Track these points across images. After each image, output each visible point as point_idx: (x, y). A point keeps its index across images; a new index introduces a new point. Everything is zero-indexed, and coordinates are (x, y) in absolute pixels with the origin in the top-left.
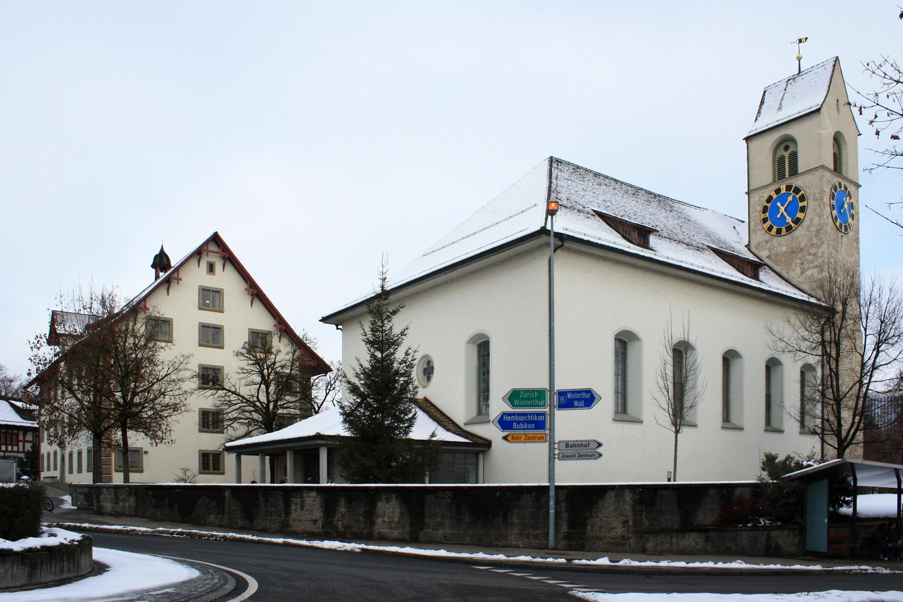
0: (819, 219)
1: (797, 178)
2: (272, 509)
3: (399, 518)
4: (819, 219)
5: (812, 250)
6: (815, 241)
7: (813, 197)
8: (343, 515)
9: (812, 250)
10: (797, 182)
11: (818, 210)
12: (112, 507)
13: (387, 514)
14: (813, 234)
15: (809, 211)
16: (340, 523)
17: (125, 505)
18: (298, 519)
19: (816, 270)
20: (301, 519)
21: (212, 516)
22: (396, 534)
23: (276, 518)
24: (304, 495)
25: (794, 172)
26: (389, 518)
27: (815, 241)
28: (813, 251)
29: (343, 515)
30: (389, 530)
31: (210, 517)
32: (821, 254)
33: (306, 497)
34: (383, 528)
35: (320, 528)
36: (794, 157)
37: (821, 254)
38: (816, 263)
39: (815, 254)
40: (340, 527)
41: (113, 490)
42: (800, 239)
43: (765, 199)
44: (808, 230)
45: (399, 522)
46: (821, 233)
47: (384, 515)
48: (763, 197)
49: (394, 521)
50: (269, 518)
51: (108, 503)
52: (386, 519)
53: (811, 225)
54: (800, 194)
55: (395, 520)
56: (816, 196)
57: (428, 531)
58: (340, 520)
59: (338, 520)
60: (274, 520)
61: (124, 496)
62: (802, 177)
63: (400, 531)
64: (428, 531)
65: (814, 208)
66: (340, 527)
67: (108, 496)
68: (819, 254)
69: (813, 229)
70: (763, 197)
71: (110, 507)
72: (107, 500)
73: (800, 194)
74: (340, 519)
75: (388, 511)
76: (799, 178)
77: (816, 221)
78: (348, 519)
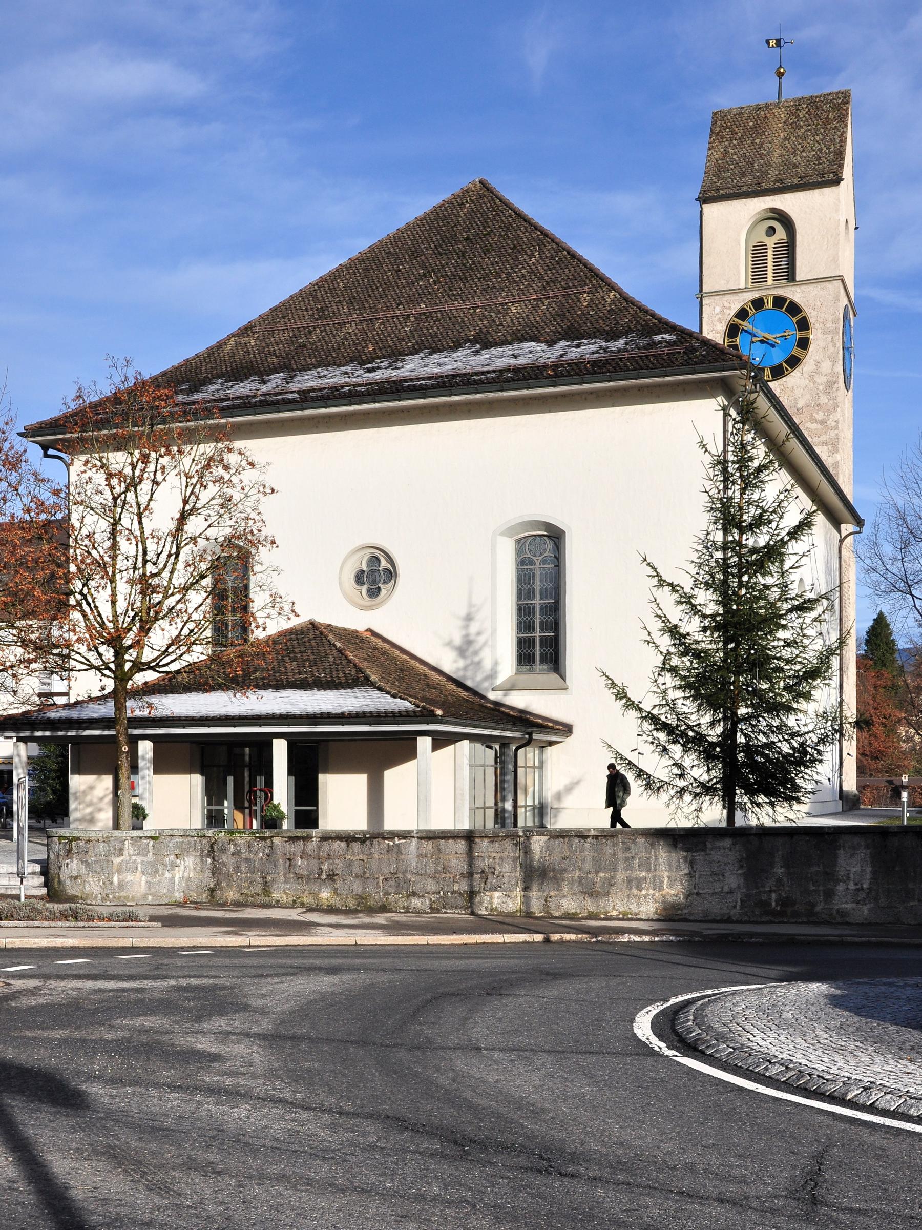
0: (831, 364)
1: (793, 289)
2: (644, 874)
3: (870, 883)
4: (831, 364)
5: (817, 413)
6: (824, 400)
7: (821, 325)
8: (779, 880)
9: (817, 413)
10: (794, 294)
11: (831, 349)
12: (149, 884)
13: (852, 876)
14: (821, 388)
15: (812, 348)
16: (774, 895)
17: (172, 879)
18: (695, 891)
19: (825, 448)
20: (701, 892)
21: (497, 894)
22: (866, 912)
23: (651, 892)
24: (709, 845)
25: (789, 274)
26: (856, 884)
27: (824, 400)
28: (820, 416)
29: (779, 880)
30: (854, 905)
31: (492, 898)
32: (834, 424)
33: (712, 849)
34: (846, 902)
35: (738, 907)
36: (789, 249)
37: (834, 424)
38: (824, 438)
39: (823, 422)
40: (774, 904)
41: (151, 842)
42: (798, 392)
43: (733, 312)
44: (812, 378)
45: (870, 889)
46: (835, 389)
47: (848, 878)
48: (730, 308)
49: (862, 889)
50: (635, 891)
51: (138, 874)
52: (852, 886)
53: (817, 371)
54: (799, 317)
55: (865, 886)
56: (828, 326)
57: (912, 904)
58: (775, 891)
59: (771, 891)
60: (645, 897)
61: (172, 857)
62: (803, 287)
63: (872, 905)
64: (912, 904)
65: (822, 344)
66: (774, 904)
67: (139, 859)
68: (831, 423)
69: (820, 380)
70: (730, 308)
71: (143, 883)
72: (137, 868)
73: (799, 317)
74: (774, 888)
75: (854, 870)
76: (798, 289)
77: (826, 366)
78: (787, 888)
